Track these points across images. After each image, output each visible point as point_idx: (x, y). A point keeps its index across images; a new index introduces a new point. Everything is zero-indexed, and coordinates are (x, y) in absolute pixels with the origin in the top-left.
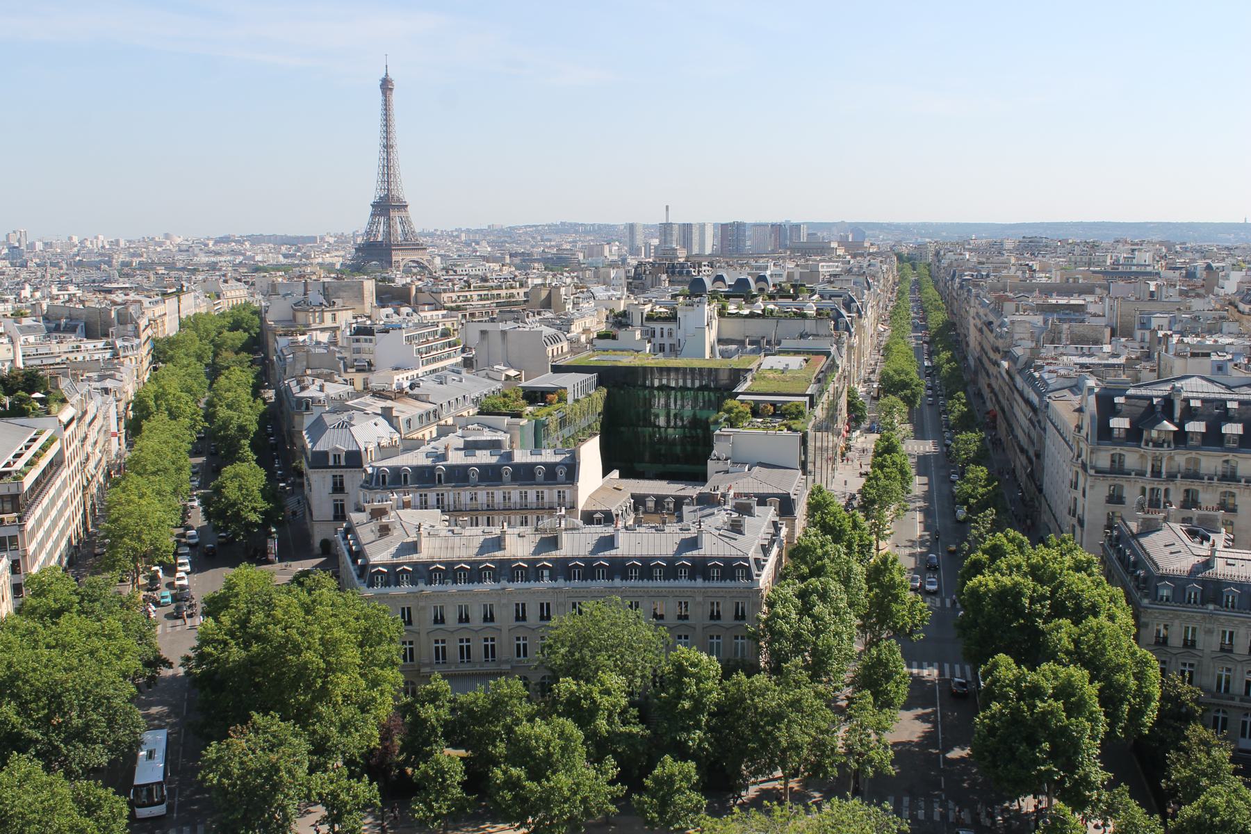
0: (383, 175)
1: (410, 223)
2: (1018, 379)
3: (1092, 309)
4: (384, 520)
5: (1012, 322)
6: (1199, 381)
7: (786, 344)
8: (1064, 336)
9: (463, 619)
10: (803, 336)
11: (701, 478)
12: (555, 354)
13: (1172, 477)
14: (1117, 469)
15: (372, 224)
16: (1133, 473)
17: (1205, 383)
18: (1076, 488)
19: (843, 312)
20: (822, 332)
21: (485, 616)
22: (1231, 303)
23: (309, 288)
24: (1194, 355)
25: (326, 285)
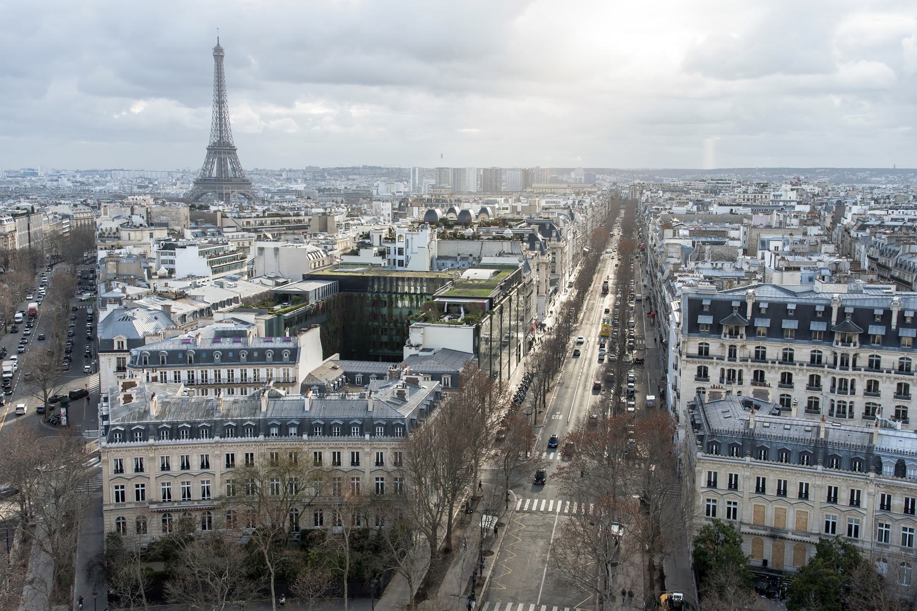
0: (216, 125)
1: (238, 164)
2: (664, 287)
3: (733, 234)
4: (129, 391)
5: (667, 244)
6: (770, 288)
7: (485, 260)
8: (706, 255)
9: (185, 466)
10: (500, 255)
11: (399, 359)
12: (317, 266)
13: (744, 360)
14: (704, 352)
15: (207, 163)
16: (715, 358)
17: (774, 289)
18: (676, 369)
19: (540, 236)
20: (515, 251)
21: (203, 464)
22: (846, 230)
23: (135, 212)
24: (788, 269)
25: (149, 210)
